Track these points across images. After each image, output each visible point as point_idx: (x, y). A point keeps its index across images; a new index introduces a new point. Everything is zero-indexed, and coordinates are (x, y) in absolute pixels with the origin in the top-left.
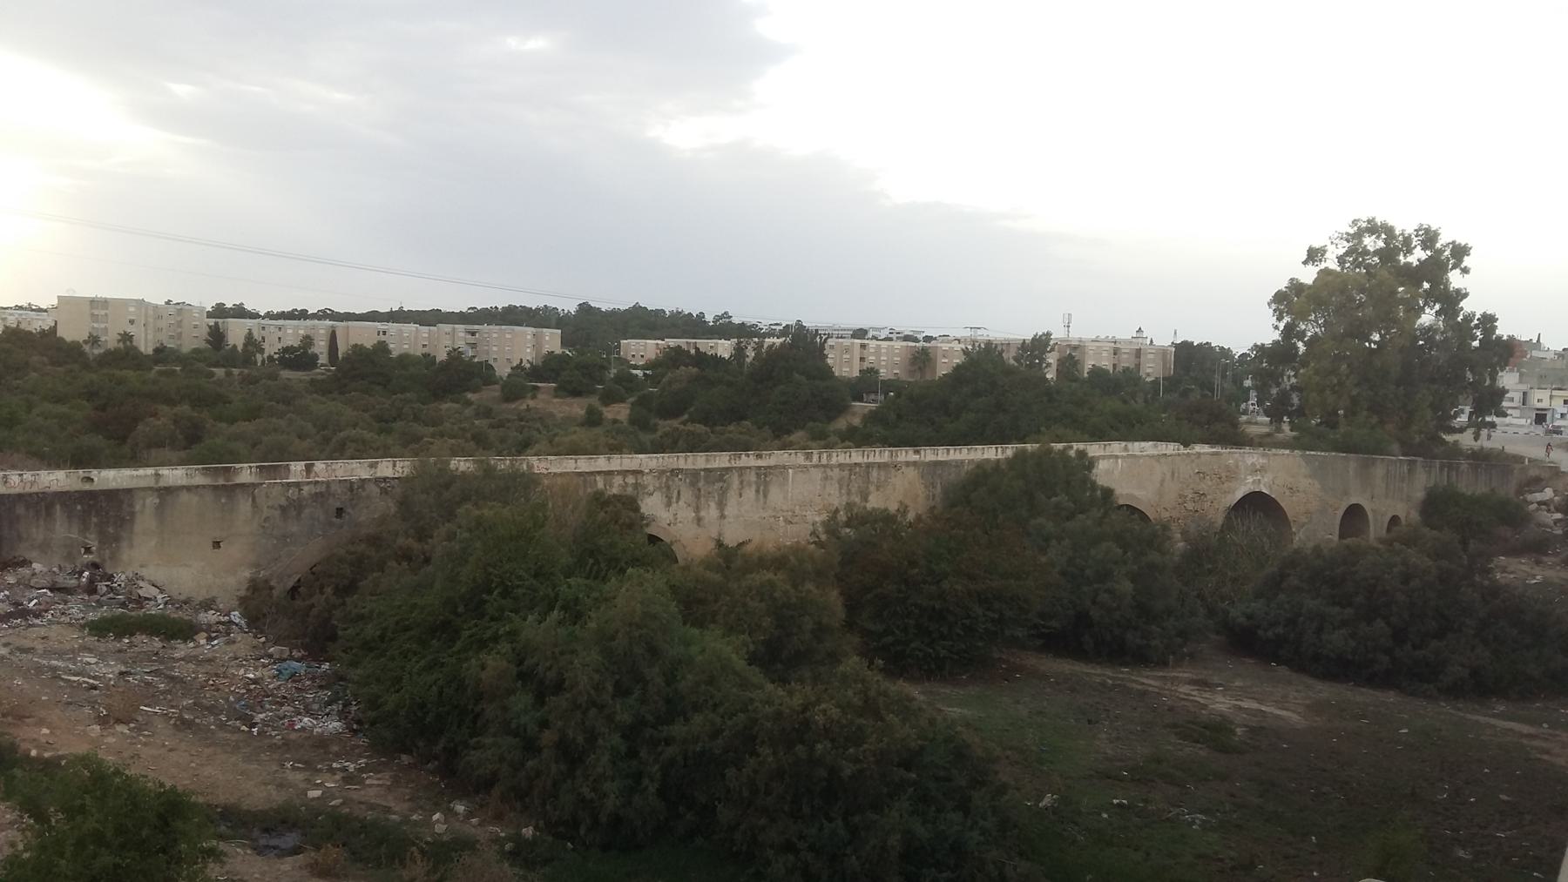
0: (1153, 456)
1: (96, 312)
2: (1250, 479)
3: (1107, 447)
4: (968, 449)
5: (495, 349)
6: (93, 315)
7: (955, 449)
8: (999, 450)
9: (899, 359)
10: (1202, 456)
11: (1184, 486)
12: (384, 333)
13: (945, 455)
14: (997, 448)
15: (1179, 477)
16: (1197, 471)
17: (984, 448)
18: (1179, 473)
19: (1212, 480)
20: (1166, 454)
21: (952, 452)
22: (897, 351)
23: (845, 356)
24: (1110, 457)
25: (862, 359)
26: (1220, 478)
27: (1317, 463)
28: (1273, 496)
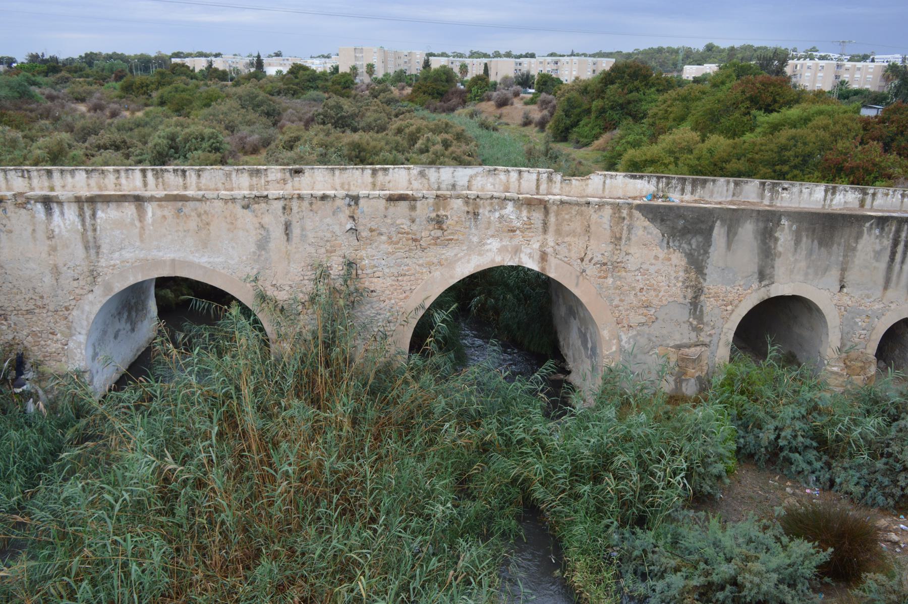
0: (234, 200)
1: (357, 55)
2: (494, 244)
3: (380, 173)
4: (87, 171)
5: (567, 73)
6: (356, 57)
7: (62, 172)
8: (150, 175)
9: (871, 76)
10: (362, 202)
11: (323, 250)
12: (520, 64)
13: (45, 178)
14: (144, 172)
15: (303, 237)
16: (348, 227)
17: (118, 171)
18: (303, 229)
19: (391, 243)
20: (267, 196)
21: (56, 175)
22: (871, 70)
23: (819, 74)
24: (123, 199)
25: (837, 77)
26: (415, 240)
27: (682, 222)
28: (552, 275)
